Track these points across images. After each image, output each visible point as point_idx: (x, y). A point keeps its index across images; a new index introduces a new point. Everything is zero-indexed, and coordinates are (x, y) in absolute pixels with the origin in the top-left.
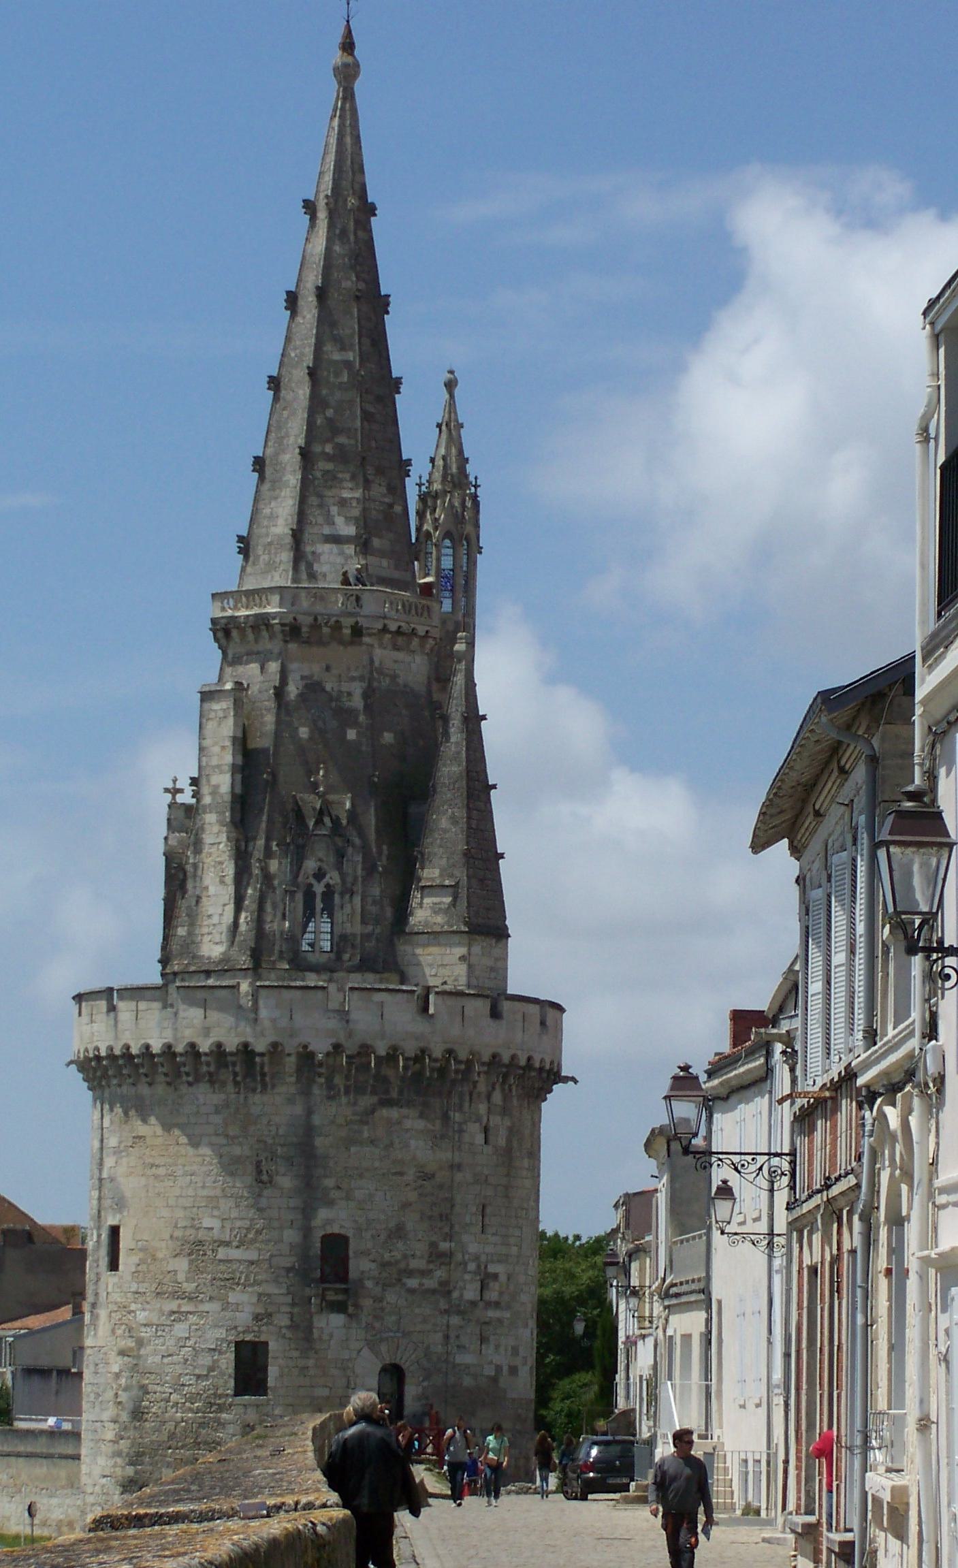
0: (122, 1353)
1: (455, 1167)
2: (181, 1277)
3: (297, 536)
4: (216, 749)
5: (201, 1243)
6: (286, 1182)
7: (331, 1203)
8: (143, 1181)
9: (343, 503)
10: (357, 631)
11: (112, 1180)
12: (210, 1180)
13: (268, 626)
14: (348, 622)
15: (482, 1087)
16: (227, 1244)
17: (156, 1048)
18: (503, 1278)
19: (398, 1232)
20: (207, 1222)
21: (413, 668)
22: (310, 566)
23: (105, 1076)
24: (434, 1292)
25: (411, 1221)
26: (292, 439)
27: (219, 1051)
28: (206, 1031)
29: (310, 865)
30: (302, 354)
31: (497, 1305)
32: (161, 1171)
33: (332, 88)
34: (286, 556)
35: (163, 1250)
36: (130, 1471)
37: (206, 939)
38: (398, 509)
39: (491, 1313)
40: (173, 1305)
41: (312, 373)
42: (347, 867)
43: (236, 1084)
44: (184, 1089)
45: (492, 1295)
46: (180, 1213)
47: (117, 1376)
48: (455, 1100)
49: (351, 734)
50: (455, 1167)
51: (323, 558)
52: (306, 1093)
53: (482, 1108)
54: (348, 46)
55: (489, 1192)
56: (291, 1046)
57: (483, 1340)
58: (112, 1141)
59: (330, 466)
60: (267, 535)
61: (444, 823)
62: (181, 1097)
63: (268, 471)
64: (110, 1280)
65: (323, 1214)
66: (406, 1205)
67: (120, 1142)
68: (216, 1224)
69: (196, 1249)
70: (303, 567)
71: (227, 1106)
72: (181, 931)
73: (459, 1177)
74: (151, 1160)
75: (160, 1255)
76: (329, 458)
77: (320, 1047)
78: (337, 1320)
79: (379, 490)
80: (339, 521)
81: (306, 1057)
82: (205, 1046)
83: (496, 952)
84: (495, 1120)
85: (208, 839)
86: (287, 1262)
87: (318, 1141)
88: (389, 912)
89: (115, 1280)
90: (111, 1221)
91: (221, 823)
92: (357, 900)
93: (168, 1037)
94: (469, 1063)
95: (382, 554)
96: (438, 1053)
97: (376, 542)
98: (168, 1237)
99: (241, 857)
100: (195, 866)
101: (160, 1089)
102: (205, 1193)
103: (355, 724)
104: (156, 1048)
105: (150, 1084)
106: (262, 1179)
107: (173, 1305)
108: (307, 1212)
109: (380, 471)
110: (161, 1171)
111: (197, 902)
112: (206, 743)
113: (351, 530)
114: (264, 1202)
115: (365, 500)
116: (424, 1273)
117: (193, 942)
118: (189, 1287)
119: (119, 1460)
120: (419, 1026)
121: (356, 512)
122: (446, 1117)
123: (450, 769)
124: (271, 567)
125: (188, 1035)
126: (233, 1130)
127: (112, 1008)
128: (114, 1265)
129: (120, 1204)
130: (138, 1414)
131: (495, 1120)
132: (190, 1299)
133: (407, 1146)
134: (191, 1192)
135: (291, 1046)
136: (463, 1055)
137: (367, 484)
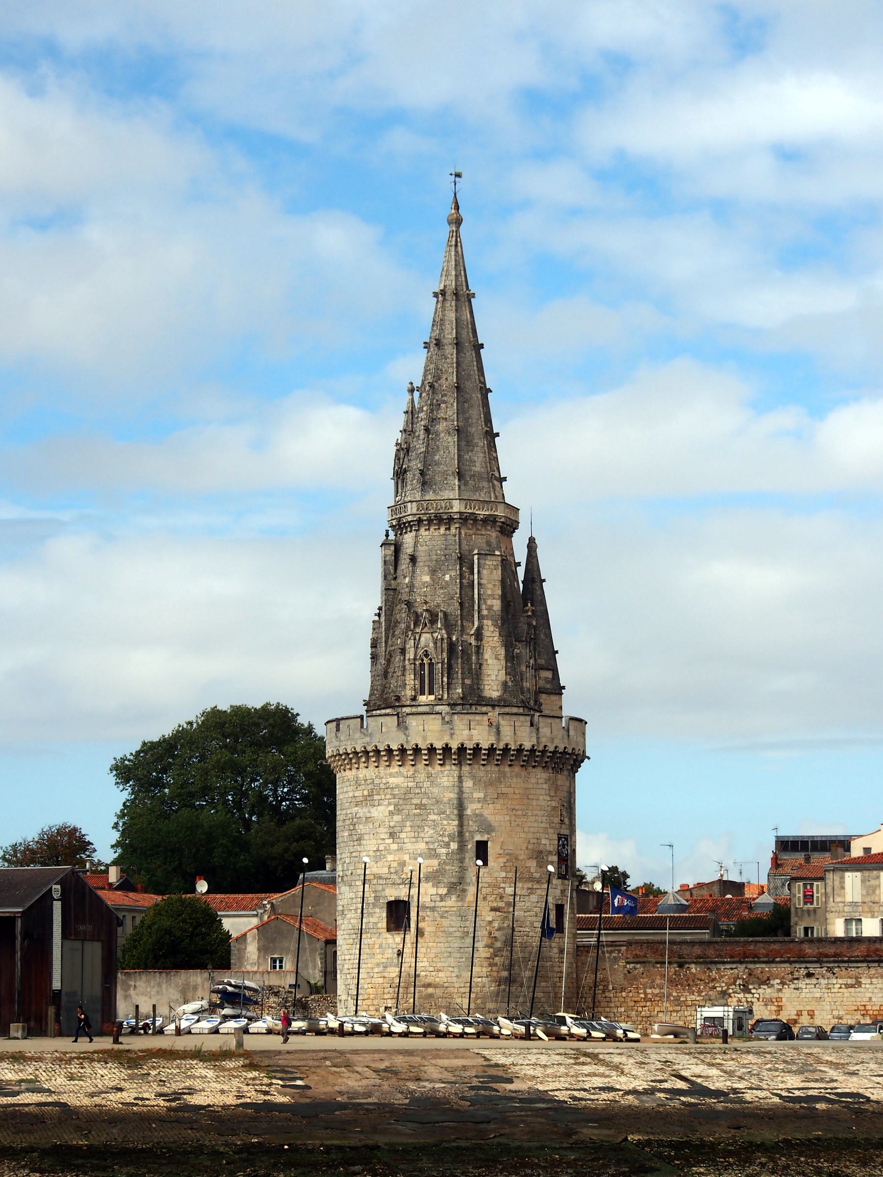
0: (493, 909)
2: (532, 870)
4: (490, 586)
5: (541, 852)
8: (507, 818)
12: (544, 818)
17: (527, 746)
20: (543, 842)
26: (474, 421)
30: (469, 375)
32: (520, 813)
33: (446, 230)
36: (505, 974)
37: (495, 688)
40: (530, 885)
43: (553, 768)
44: (530, 769)
47: (490, 922)
54: (457, 207)
60: (470, 470)
62: (529, 773)
67: (485, 796)
71: (549, 780)
74: (513, 807)
75: (521, 858)
85: (486, 633)
89: (487, 870)
90: (478, 838)
91: (495, 626)
93: (493, 740)
98: (524, 848)
100: (478, 648)
101: (517, 769)
102: (543, 825)
104: (527, 746)
105: (510, 765)
107: (530, 885)
110: (520, 813)
111: (480, 668)
112: (482, 581)
117: (479, 689)
118: (537, 875)
119: (494, 968)
125: (544, 741)
129: (488, 828)
130: (510, 942)
132: (538, 882)
134: (536, 825)
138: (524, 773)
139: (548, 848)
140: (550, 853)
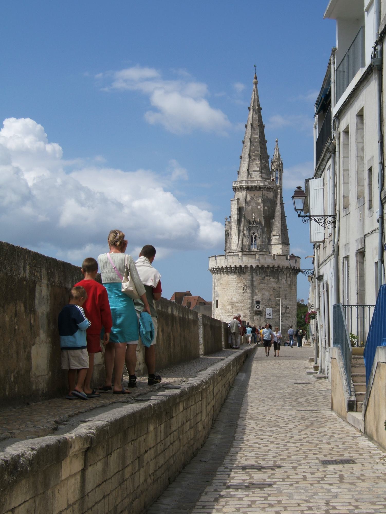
1: (280, 288)
3: (248, 170)
6: (249, 291)
7: (257, 295)
9: (257, 164)
10: (260, 188)
11: (216, 291)
13: (243, 187)
14: (258, 186)
15: (285, 273)
16: (238, 303)
18: (290, 308)
19: (270, 300)
21: (271, 195)
22: (251, 176)
23: (215, 272)
24: (277, 311)
25: (272, 298)
27: (235, 267)
28: (233, 263)
29: (252, 232)
31: (289, 313)
34: (246, 174)
35: (226, 304)
38: (267, 165)
39: (288, 315)
40: (228, 314)
41: (250, 140)
42: (259, 232)
45: (288, 311)
46: (229, 297)
48: (280, 275)
49: (259, 207)
50: (280, 288)
51: (253, 174)
52: (252, 274)
53: (285, 276)
54: (256, 78)
55: (287, 292)
56: (249, 266)
57: (286, 320)
58: (216, 284)
59: (254, 157)
61: (277, 223)
63: (242, 158)
64: (217, 309)
65: (255, 297)
66: (271, 295)
68: (236, 299)
69: (232, 304)
70: (249, 176)
72: (228, 245)
73: (281, 289)
76: (254, 156)
77: (254, 266)
78: (259, 316)
79: (263, 161)
80: (256, 167)
81: (252, 267)
82: (232, 266)
83: (287, 247)
84: (288, 279)
85: (233, 227)
86: (249, 306)
87: (254, 283)
88: (267, 240)
91: (235, 224)
92: (261, 238)
94: (282, 268)
95: (264, 173)
96: (276, 267)
97: (263, 171)
99: (239, 231)
103: (260, 205)
104: (224, 267)
106: (244, 291)
107: (228, 314)
108: (252, 297)
109: (263, 158)
113: (258, 169)
114: (244, 295)
115: (261, 163)
116: (275, 308)
118: (231, 311)
120: (273, 262)
121: (259, 165)
122: (278, 279)
123: (278, 213)
124: (243, 176)
125: (230, 264)
126: (239, 281)
127: (216, 259)
128: (217, 307)
131: (288, 279)
133: (271, 284)
135: (249, 266)
136: (281, 267)
137: (261, 160)
138: (226, 275)
139: (236, 301)
140: (238, 303)
